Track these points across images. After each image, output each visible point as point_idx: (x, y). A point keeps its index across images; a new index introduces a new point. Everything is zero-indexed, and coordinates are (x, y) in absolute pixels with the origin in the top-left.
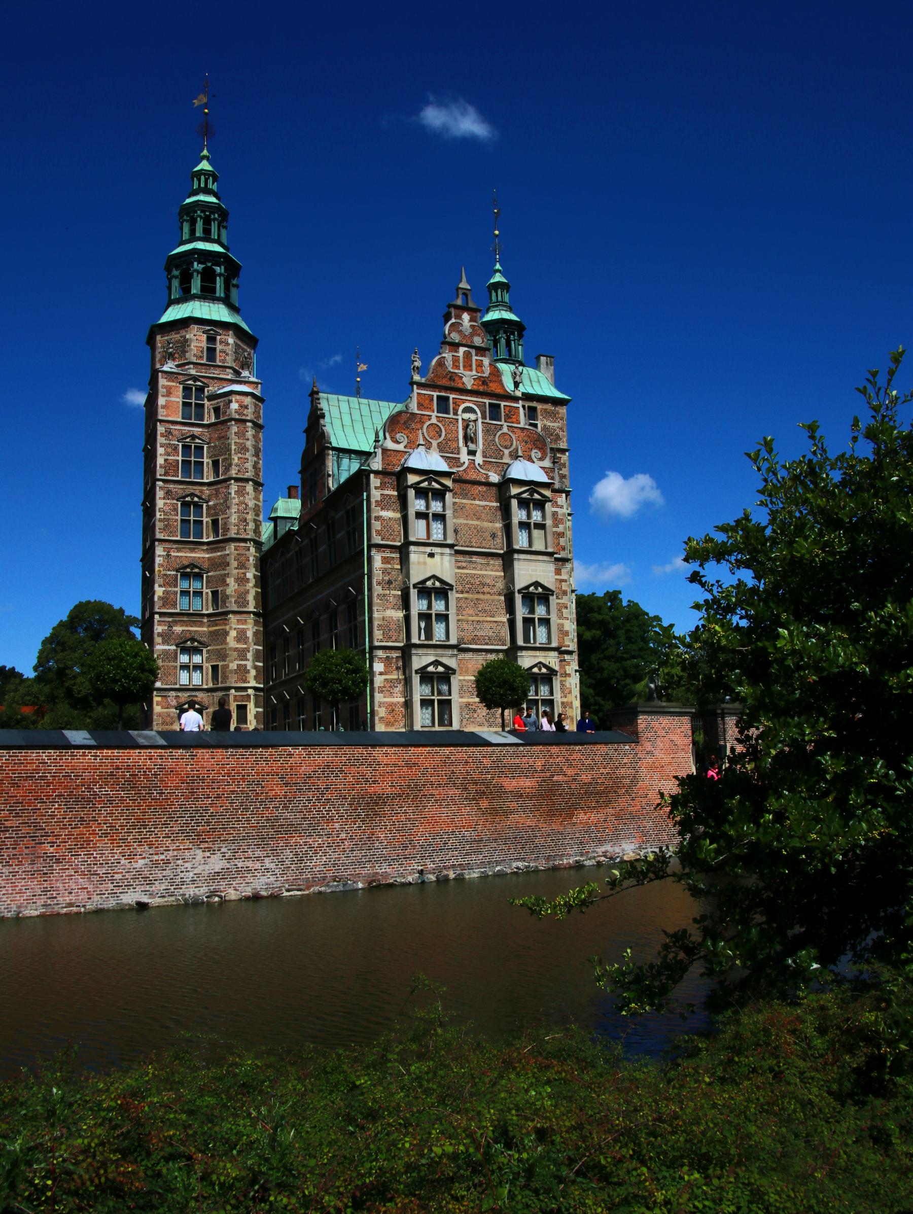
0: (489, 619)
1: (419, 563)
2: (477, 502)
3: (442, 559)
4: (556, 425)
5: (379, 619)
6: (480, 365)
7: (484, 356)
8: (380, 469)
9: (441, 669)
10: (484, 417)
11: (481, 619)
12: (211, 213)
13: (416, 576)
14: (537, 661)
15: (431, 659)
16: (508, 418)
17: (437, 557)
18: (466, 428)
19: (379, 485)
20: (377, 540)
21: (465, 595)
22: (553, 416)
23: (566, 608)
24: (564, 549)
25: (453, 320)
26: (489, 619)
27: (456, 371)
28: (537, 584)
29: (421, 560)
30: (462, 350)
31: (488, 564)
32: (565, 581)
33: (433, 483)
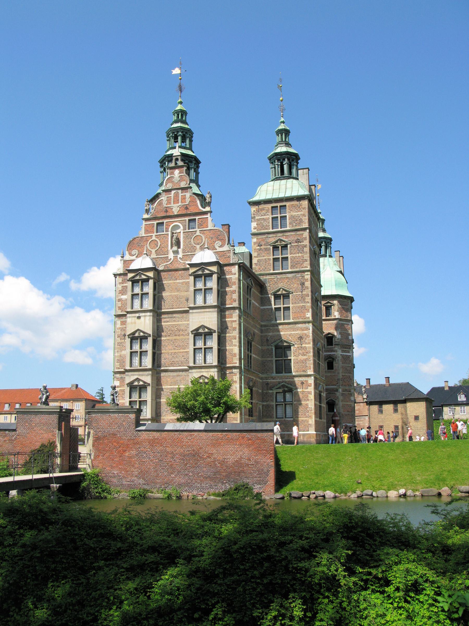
0: (182, 351)
1: (132, 323)
2: (178, 281)
3: (145, 319)
4: (299, 213)
5: (118, 356)
6: (184, 198)
7: (187, 192)
8: (122, 273)
9: (141, 383)
10: (184, 229)
11: (177, 351)
12: (178, 132)
13: (130, 331)
14: (202, 374)
15: (135, 377)
16: (200, 225)
17: (142, 318)
18: (172, 237)
19: (121, 281)
20: (120, 313)
21: (168, 338)
22: (299, 208)
23: (235, 338)
24: (235, 301)
25: (169, 176)
26: (182, 351)
27: (169, 206)
28: (203, 327)
29: (133, 321)
30: (173, 192)
31: (183, 317)
32: (235, 321)
33: (142, 276)
